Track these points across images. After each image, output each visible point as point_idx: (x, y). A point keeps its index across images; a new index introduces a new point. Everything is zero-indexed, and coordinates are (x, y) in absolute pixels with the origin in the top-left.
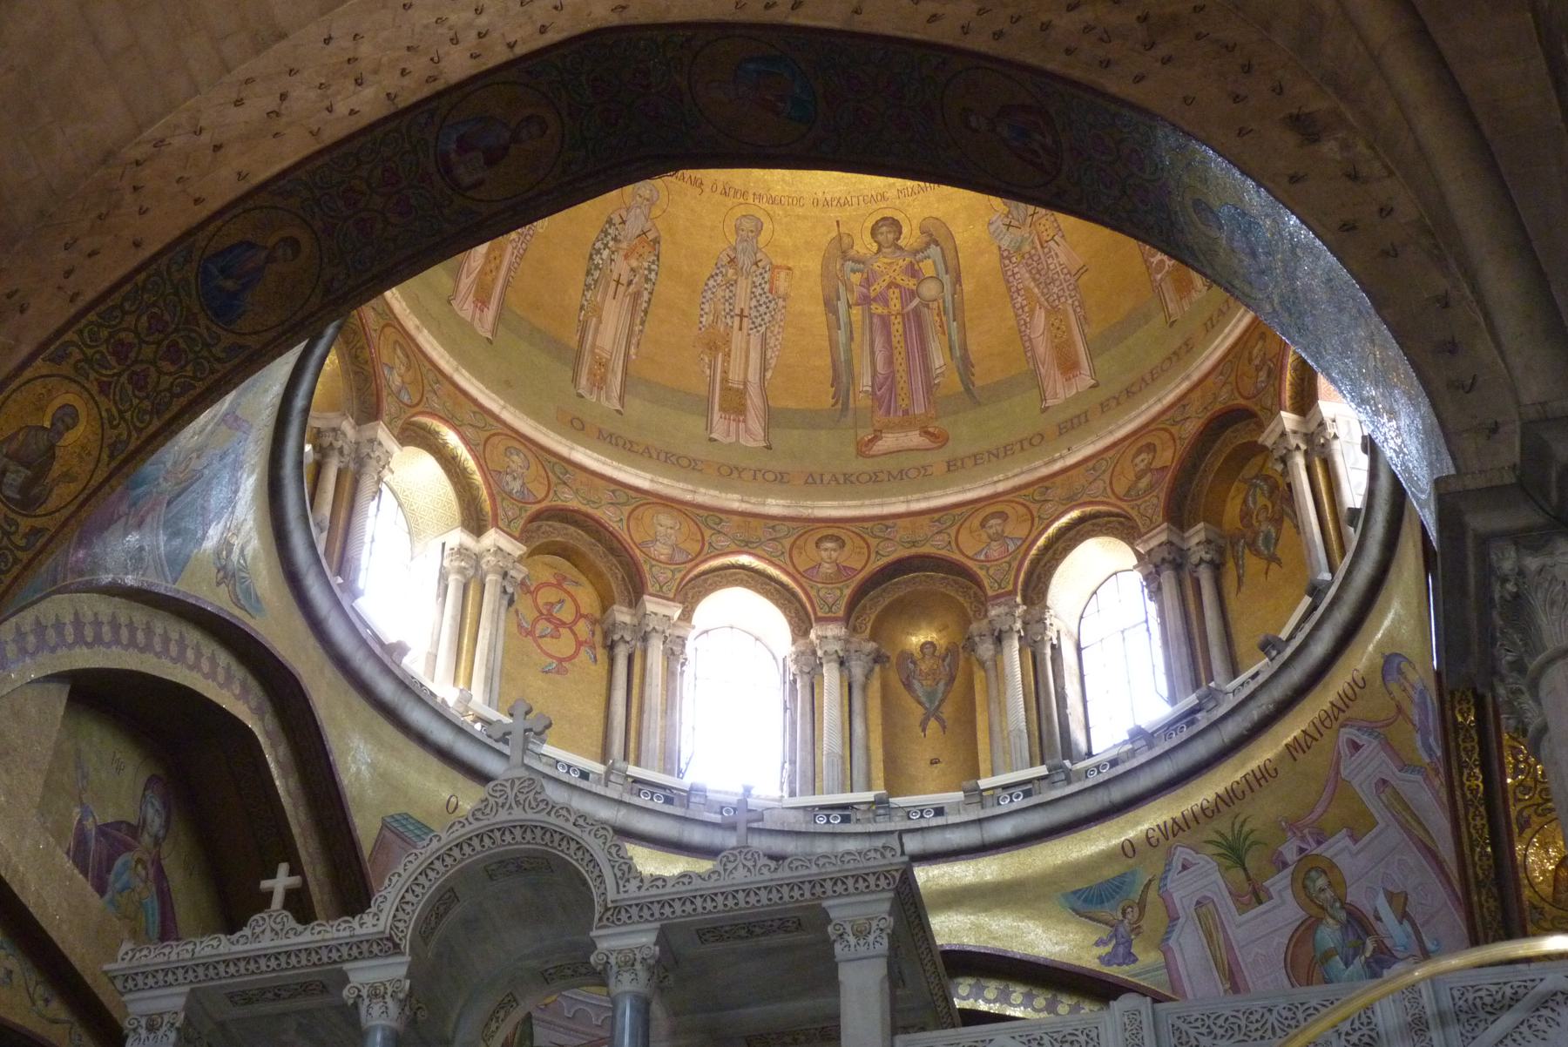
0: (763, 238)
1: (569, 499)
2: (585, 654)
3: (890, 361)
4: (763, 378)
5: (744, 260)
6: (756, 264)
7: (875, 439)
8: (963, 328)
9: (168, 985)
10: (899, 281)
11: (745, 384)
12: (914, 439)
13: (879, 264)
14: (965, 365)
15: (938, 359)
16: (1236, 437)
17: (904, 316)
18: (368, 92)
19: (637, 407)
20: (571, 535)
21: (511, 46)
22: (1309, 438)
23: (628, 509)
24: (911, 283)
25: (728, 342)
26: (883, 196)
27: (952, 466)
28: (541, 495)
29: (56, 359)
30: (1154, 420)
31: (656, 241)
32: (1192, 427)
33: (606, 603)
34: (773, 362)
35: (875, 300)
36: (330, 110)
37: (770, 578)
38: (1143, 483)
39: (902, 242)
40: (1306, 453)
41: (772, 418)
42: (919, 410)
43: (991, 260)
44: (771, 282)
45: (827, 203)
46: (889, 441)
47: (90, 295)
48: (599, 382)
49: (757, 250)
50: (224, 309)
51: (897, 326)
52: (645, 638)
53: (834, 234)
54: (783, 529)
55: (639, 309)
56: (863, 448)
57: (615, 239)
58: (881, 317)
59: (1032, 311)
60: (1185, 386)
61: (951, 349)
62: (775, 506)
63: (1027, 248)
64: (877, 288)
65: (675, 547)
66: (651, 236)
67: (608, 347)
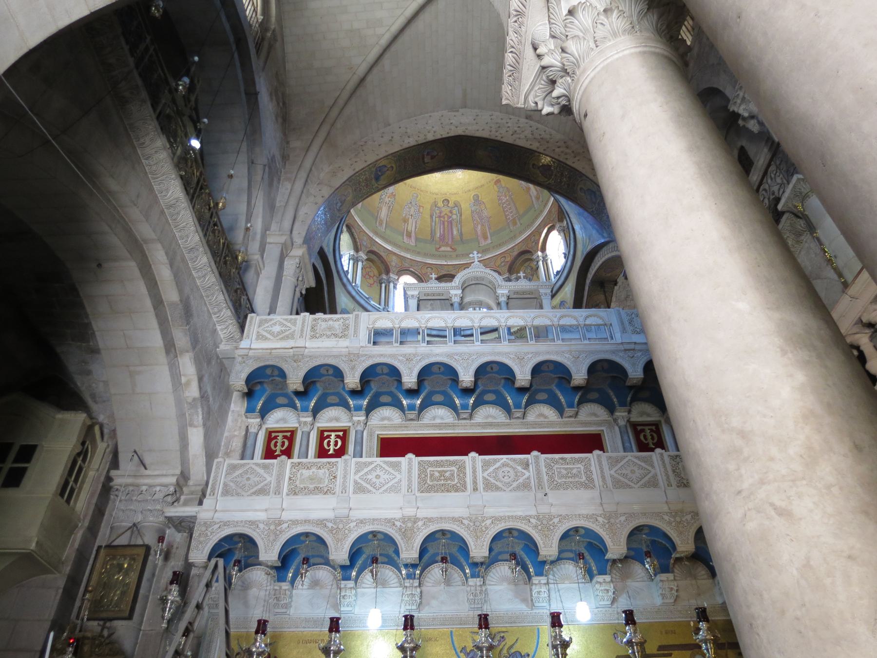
1: (375, 249)
3: (444, 231)
5: (413, 203)
8: (461, 226)
12: (449, 249)
13: (443, 209)
14: (461, 234)
15: (455, 232)
16: (527, 256)
18: (411, 139)
19: (388, 232)
20: (373, 257)
22: (543, 258)
24: (450, 215)
27: (457, 256)
29: (350, 182)
32: (516, 253)
36: (404, 142)
38: (503, 264)
41: (417, 239)
42: (450, 243)
46: (443, 249)
47: (357, 170)
48: (381, 224)
50: (377, 178)
51: (446, 224)
52: (389, 283)
54: (419, 264)
55: (390, 210)
56: (437, 249)
60: (514, 245)
62: (419, 259)
64: (442, 214)
65: (396, 264)
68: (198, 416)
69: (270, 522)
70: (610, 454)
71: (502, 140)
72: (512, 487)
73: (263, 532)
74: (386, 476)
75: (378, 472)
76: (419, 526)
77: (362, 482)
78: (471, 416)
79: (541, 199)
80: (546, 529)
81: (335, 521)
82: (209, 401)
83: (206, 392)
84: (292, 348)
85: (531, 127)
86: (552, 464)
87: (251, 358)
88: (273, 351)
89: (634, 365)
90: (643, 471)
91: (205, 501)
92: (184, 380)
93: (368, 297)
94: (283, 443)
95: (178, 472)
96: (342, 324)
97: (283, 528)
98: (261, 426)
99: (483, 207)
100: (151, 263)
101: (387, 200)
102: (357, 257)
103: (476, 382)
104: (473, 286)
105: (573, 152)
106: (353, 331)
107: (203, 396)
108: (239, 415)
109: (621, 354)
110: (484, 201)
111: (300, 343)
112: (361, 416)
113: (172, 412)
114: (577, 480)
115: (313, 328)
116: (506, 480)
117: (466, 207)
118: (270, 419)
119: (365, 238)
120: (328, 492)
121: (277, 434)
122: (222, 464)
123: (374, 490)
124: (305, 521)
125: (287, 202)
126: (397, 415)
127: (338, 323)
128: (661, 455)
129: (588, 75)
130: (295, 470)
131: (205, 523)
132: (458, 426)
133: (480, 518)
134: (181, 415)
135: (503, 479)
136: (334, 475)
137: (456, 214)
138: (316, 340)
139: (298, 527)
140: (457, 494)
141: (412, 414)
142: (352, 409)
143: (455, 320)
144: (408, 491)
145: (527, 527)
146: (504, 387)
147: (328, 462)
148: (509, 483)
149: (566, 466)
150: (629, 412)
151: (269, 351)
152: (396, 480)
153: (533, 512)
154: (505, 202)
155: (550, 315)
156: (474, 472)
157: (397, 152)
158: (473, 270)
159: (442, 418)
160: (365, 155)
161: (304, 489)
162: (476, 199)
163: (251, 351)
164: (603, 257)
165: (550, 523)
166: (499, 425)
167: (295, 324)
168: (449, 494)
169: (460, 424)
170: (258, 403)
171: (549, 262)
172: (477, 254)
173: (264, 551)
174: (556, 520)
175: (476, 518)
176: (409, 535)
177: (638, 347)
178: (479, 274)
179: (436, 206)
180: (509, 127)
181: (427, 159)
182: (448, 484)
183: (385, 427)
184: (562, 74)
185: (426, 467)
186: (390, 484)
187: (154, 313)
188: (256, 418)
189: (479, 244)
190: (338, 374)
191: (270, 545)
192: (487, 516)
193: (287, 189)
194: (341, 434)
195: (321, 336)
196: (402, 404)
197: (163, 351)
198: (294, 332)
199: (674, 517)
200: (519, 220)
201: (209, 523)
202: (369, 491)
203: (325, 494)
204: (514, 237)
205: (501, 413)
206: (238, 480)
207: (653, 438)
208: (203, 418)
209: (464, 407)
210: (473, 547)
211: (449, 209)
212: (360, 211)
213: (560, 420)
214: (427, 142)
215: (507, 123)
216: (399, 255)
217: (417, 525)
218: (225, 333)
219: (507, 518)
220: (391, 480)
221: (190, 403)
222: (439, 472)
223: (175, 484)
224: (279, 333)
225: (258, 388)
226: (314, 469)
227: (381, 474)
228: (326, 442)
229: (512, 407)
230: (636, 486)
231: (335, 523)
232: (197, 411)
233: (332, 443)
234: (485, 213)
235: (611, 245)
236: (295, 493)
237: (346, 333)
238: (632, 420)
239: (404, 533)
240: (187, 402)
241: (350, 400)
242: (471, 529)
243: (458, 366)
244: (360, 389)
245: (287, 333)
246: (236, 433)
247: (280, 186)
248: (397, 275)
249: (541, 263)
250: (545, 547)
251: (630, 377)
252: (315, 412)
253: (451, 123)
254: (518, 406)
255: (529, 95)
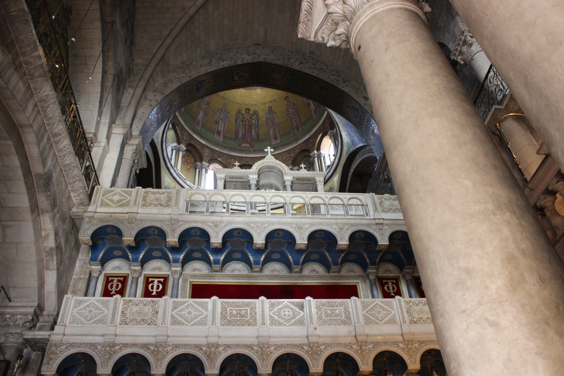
0: (227, 107)
1: (192, 142)
2: (192, 168)
3: (245, 132)
4: (224, 130)
6: (225, 111)
7: (242, 144)
8: (258, 129)
9: (222, 173)
10: (248, 119)
11: (221, 130)
12: (248, 145)
13: (246, 116)
14: (258, 135)
15: (253, 133)
16: (307, 154)
17: (249, 125)
18: (225, 63)
19: (203, 130)
21: (248, 61)
22: (318, 155)
23: (201, 147)
24: (250, 120)
25: (219, 123)
26: (248, 105)
28: (189, 140)
30: (291, 149)
31: (210, 103)
32: (297, 151)
33: (196, 161)
34: (226, 128)
35: (244, 121)
37: (222, 163)
38: (288, 159)
39: (250, 113)
40: (317, 158)
41: (225, 137)
42: (249, 141)
43: (264, 119)
44: (227, 115)
45: (238, 104)
46: (244, 145)
47: (183, 82)
48: (198, 124)
49: (226, 109)
50: (198, 90)
51: (247, 126)
52: (202, 168)
53: (239, 109)
54: (225, 155)
57: (203, 101)
58: (245, 124)
59: (270, 129)
60: (297, 144)
61: (256, 132)
63: (271, 118)
64: (245, 119)
66: (209, 102)
67: (200, 119)
68: (53, 262)
69: (106, 344)
70: (363, 299)
71: (292, 67)
72: (291, 322)
73: (100, 352)
74: (196, 313)
75: (190, 309)
76: (220, 350)
77: (178, 317)
78: (261, 270)
79: (318, 112)
80: (315, 354)
81: (156, 345)
82: (62, 251)
83: (60, 243)
84: (127, 213)
85: (313, 60)
86: (321, 307)
87: (96, 219)
88: (113, 215)
89: (382, 235)
90: (386, 312)
91: (56, 327)
92: (43, 233)
93: (185, 178)
94: (118, 285)
95: (36, 304)
96: (166, 197)
97: (116, 349)
98: (101, 272)
99: (275, 115)
100: (24, 143)
101: (204, 106)
102: (179, 148)
103: (266, 244)
104: (266, 173)
105: (343, 79)
106: (174, 202)
107: (58, 247)
108: (84, 263)
109: (374, 227)
110: (276, 111)
111: (135, 210)
112: (178, 267)
113: (33, 258)
114: (339, 318)
115: (144, 199)
116: (287, 317)
117: (262, 114)
118: (108, 267)
119: (186, 134)
120: (151, 323)
121: (113, 278)
122: (70, 300)
123: (186, 323)
124: (133, 345)
125: (129, 103)
126: (206, 267)
127: (163, 196)
128: (399, 300)
129: (362, 20)
130: (126, 306)
131: (55, 344)
132: (251, 277)
133: (266, 345)
134: (40, 261)
135: (284, 317)
136: (156, 311)
137: (255, 120)
138: (146, 207)
139: (128, 349)
140: (249, 327)
141: (217, 267)
142: (172, 262)
143: (252, 197)
144: (212, 325)
145: (301, 352)
146: (287, 249)
147: (152, 301)
148: (289, 320)
149: (331, 308)
150: (377, 269)
151: (110, 215)
152: (203, 316)
153: (305, 341)
154: (291, 113)
155: (323, 196)
156: (263, 311)
157: (214, 71)
158: (267, 161)
159: (239, 271)
160: (190, 72)
161: (132, 321)
162: (270, 109)
163: (96, 214)
164: (362, 156)
165: (318, 349)
166: (282, 277)
167: (130, 195)
168: (243, 327)
169: (253, 276)
170: (99, 254)
171: (322, 158)
172: (270, 149)
173: (100, 367)
174: (322, 347)
175: (264, 345)
176: (212, 357)
177: (385, 222)
178: (271, 164)
179: (240, 113)
180: (297, 59)
181: (236, 78)
182: (243, 320)
183: (195, 276)
184: (343, 18)
185: (227, 307)
186: (199, 319)
187: (24, 181)
188: (98, 265)
189: (271, 143)
190: (162, 234)
191: (106, 362)
192: (271, 344)
193: (130, 94)
194: (162, 280)
195: (150, 205)
196: (210, 259)
197: (29, 210)
198: (129, 201)
199: (407, 345)
200: (301, 127)
201: (58, 344)
202: (183, 324)
203: (149, 325)
204: (297, 140)
205: (284, 268)
206: (83, 311)
207: (393, 289)
208: (57, 264)
209: (257, 263)
210: (261, 367)
211: (249, 116)
212: (183, 113)
213: (327, 274)
214: (237, 65)
215: (296, 55)
216: (211, 148)
217: (218, 350)
218: (77, 199)
219: (286, 346)
220: (200, 316)
221: (47, 252)
222: (236, 310)
223: (33, 313)
224: (118, 201)
225: (100, 242)
226: (141, 306)
227: (192, 311)
228: (150, 285)
229: (292, 264)
230: (381, 323)
231: (156, 347)
232: (53, 258)
233: (155, 287)
234: (277, 120)
235: (367, 148)
236: (126, 323)
237: (169, 203)
238: (379, 275)
239: (209, 356)
240: (45, 251)
241: (170, 254)
242: (259, 353)
243: (253, 231)
244: (178, 246)
245: (124, 202)
246: (82, 276)
247: (125, 91)
248: (208, 163)
249: (316, 159)
250: (314, 367)
251: (379, 244)
252: (143, 263)
253: (255, 53)
254: (297, 263)
255: (318, 32)
